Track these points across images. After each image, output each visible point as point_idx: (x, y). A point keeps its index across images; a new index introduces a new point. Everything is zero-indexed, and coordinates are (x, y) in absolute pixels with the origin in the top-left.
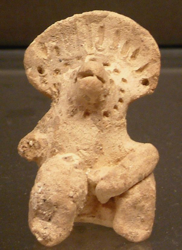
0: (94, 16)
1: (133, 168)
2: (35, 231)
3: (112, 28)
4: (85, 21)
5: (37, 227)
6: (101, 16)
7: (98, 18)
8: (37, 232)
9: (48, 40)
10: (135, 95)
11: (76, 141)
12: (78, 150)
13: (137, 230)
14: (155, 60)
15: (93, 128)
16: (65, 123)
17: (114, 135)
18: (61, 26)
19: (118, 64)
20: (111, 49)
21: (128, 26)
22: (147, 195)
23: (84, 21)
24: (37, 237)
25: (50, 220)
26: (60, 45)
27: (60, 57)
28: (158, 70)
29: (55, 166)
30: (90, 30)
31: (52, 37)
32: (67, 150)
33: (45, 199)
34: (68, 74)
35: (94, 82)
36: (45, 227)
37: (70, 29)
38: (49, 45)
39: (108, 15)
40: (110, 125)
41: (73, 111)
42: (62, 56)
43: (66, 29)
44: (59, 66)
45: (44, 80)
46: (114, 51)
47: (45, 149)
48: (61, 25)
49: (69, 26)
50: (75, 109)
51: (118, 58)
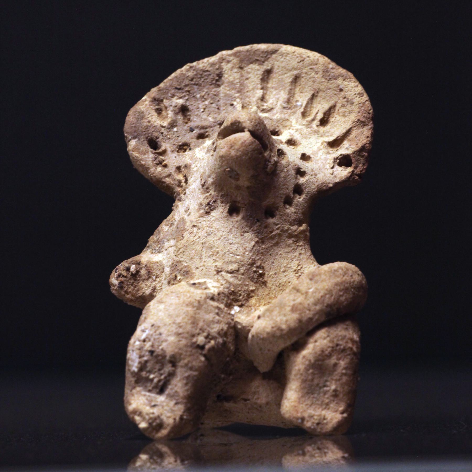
0: (254, 52)
1: (315, 293)
2: (135, 412)
3: (286, 72)
4: (238, 62)
5: (139, 404)
6: (266, 52)
7: (261, 55)
8: (138, 413)
9: (170, 95)
10: (325, 181)
11: (214, 258)
12: (218, 272)
13: (324, 412)
14: (362, 122)
15: (246, 235)
16: (194, 226)
17: (286, 250)
18: (194, 70)
19: (298, 133)
20: (284, 108)
21: (316, 65)
22: (341, 345)
23: (235, 60)
24: (138, 422)
25: (161, 390)
26: (191, 103)
27: (191, 124)
28: (369, 139)
29: (174, 294)
30: (247, 77)
31: (177, 90)
32: (197, 273)
33: (153, 349)
34: (204, 148)
35: (245, 141)
36: (153, 404)
37: (211, 77)
38: (172, 102)
39: (280, 49)
40: (278, 232)
41: (208, 204)
42: (195, 121)
43: (203, 76)
44: (188, 137)
45: (160, 160)
46: (289, 111)
47: (158, 280)
48: (194, 68)
49: (207, 71)
50: (214, 200)
51: (297, 122)
